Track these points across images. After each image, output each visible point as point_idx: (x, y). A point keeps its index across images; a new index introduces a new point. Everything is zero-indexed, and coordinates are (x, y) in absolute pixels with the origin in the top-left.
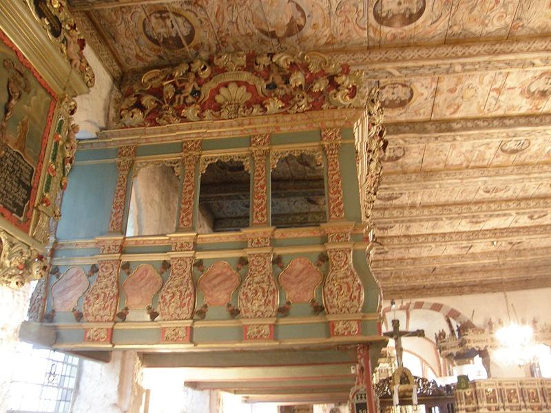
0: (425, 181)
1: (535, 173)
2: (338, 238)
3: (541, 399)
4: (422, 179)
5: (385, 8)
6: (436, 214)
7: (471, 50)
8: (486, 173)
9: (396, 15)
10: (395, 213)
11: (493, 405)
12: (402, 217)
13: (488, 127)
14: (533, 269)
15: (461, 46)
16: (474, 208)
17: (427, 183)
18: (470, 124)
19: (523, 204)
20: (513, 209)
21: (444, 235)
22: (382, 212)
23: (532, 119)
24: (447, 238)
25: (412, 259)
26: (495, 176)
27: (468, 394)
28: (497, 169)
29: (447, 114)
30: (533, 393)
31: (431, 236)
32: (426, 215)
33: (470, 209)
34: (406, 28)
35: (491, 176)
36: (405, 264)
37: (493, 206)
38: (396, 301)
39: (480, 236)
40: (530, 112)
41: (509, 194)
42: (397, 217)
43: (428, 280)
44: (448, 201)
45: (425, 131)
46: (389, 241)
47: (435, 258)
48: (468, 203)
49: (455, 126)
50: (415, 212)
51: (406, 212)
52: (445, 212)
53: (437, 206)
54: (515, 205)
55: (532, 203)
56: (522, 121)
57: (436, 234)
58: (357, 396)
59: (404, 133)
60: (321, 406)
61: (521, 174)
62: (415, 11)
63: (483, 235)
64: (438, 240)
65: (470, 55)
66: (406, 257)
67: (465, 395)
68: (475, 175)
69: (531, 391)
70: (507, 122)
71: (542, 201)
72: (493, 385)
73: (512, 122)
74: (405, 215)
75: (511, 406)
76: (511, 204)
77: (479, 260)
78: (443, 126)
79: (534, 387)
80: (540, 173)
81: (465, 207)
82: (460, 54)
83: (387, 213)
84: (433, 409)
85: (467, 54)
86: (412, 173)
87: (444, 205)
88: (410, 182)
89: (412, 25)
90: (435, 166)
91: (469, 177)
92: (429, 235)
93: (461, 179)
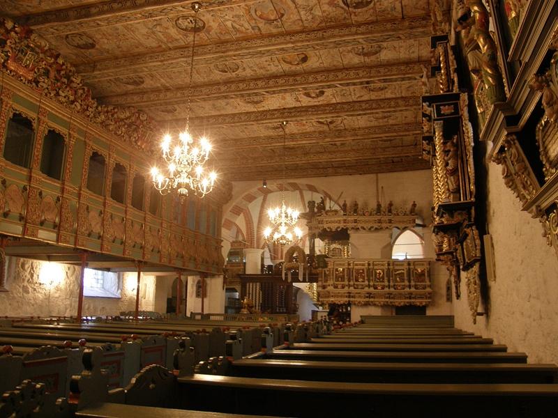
1: (231, 50)
3: (386, 278)
8: (186, 53)
10: (152, 96)
11: (340, 283)
12: (158, 100)
14: (380, 150)
16: (223, 88)
17: (133, 67)
18: (106, 8)
19: (271, 83)
20: (262, 88)
21: (234, 115)
22: (141, 96)
27: (327, 273)
30: (380, 274)
33: (219, 89)
37: (241, 86)
38: (268, 182)
39: (268, 117)
41: (248, 73)
42: (153, 100)
43: (273, 161)
45: (67, 18)
48: (218, 84)
49: (94, 10)
50: (169, 94)
51: (162, 96)
54: (264, 83)
55: (281, 81)
57: (227, 115)
60: (192, 277)
61: (219, 52)
67: (325, 273)
68: (175, 56)
69: (378, 272)
71: (291, 79)
72: (344, 265)
75: (357, 285)
76: (259, 82)
77: (297, 141)
78: (83, 12)
79: (382, 267)
80: (236, 50)
83: (145, 96)
86: (121, 58)
93: (162, 61)
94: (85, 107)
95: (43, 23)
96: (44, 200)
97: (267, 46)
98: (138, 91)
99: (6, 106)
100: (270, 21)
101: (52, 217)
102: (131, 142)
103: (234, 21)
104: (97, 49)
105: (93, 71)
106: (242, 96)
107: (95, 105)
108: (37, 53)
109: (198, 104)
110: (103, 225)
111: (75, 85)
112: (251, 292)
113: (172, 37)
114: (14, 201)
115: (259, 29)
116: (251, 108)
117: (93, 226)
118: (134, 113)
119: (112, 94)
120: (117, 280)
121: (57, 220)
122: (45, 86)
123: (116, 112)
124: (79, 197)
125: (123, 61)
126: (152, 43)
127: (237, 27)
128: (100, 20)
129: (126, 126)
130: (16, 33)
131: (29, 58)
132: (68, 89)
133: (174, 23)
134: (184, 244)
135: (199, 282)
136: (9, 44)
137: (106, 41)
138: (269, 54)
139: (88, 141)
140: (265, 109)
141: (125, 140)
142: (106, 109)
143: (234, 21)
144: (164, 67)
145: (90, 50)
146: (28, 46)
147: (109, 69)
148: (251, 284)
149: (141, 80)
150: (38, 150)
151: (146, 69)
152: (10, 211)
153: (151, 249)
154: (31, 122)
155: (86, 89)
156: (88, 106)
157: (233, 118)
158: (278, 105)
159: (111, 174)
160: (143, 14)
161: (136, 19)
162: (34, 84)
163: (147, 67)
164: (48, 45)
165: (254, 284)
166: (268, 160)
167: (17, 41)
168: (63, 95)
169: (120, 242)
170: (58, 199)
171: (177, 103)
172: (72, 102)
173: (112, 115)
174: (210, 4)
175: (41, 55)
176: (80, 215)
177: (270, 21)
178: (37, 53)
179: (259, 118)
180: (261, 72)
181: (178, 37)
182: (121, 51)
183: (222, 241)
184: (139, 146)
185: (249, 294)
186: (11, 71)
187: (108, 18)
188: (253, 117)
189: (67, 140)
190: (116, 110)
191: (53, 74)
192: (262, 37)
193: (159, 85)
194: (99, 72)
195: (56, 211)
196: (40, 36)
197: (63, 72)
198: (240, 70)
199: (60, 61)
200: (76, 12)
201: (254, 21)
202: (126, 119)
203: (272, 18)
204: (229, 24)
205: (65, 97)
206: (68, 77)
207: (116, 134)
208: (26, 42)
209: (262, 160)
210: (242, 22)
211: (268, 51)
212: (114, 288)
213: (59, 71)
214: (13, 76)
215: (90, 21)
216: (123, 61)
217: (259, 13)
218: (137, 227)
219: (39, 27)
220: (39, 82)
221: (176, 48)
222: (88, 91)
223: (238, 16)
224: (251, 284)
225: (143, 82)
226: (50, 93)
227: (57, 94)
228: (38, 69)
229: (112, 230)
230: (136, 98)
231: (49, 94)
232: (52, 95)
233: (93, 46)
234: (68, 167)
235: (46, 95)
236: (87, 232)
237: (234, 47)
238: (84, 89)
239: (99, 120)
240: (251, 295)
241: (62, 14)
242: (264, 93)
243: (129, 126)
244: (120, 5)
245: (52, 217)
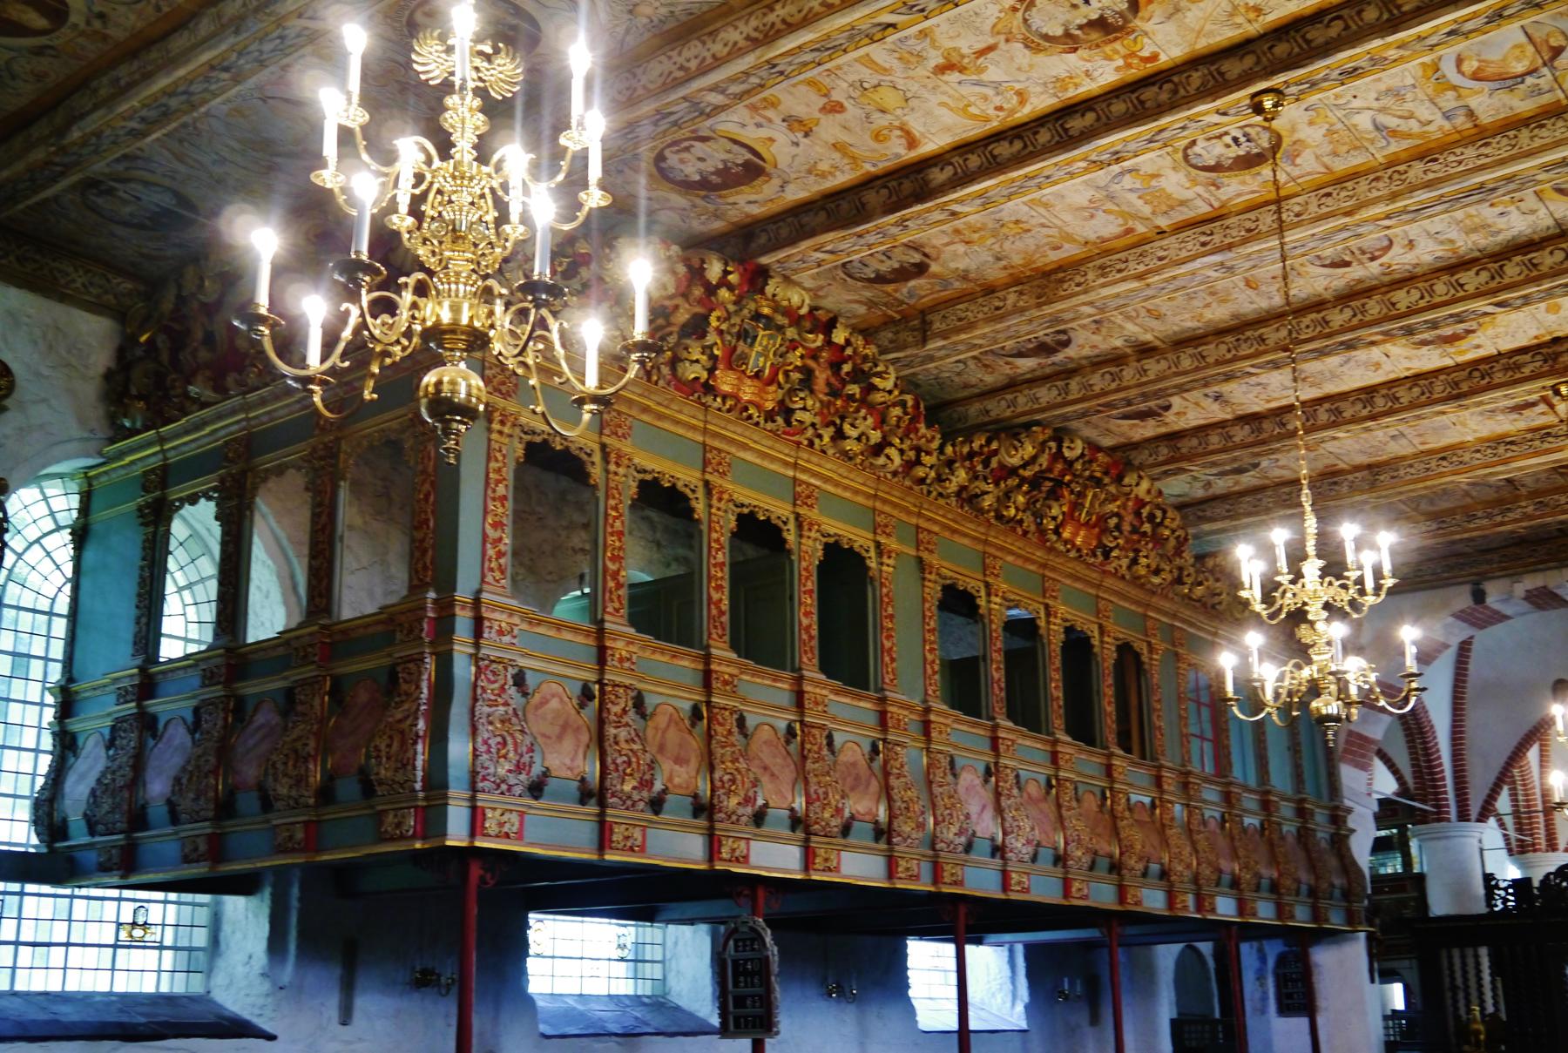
0: (1039, 306)
2: (411, 631)
4: (1033, 301)
6: (1218, 363)
7: (718, 48)
8: (1217, 238)
10: (1098, 381)
13: (1019, 160)
15: (698, 38)
17: (1047, 310)
18: (974, 161)
19: (1512, 270)
20: (1479, 294)
21: (1370, 391)
23: (1149, 94)
24: (1380, 403)
25: (1369, 467)
26: (1245, 241)
28: (1252, 215)
29: (898, 152)
31: (1327, 406)
32: (1185, 373)
35: (1230, 247)
36: (1345, 489)
37: (1403, 298)
39: (1499, 377)
40: (1134, 73)
42: (1104, 393)
43: (1511, 515)
44: (1360, 281)
45: (862, 215)
46: (1195, 442)
47: (1444, 453)
49: (938, 176)
50: (1153, 367)
51: (1128, 374)
52: (1245, 350)
53: (1220, 332)
56: (1118, 107)
57: (1343, 396)
58: (736, 941)
59: (812, 234)
63: (1506, 369)
64: (1347, 415)
65: (718, 62)
66: (1342, 466)
68: (1184, 254)
70: (1076, 124)
73: (1090, 117)
74: (1125, 384)
80: (1394, 197)
81: (1306, 320)
82: (693, 65)
83: (1074, 384)
84: (1444, 954)
85: (709, 60)
86: (1007, 286)
87: (1240, 328)
88: (1002, 318)
90: (1054, 257)
91: (1166, 262)
92: (1319, 401)
94: (912, 454)
95: (792, 241)
96: (842, 758)
97: (1502, 162)
98: (1048, 370)
100: (1510, 81)
101: (866, 805)
102: (1042, 532)
103: (1382, 110)
104: (935, 276)
105: (924, 341)
106: (1409, 331)
107: (935, 444)
108: (780, 329)
109: (1253, 380)
110: (999, 811)
111: (878, 397)
112: (1459, 981)
113: (1169, 197)
114: (773, 775)
115: (1471, 114)
116: (1431, 359)
117: (974, 817)
118: (1043, 444)
119: (966, 393)
120: (1008, 973)
121: (882, 814)
122: (807, 417)
123: (996, 452)
124: (927, 732)
125: (1012, 298)
126: (1105, 227)
127: (1392, 122)
128: (955, 201)
129: (1025, 488)
130: (731, 288)
131: (761, 353)
132: (863, 412)
133: (1180, 155)
134: (1232, 839)
135: (1281, 961)
136: (714, 323)
137: (961, 248)
138: (1512, 186)
139: (925, 555)
140: (1481, 353)
141: (1025, 533)
142: (966, 450)
143: (1382, 110)
144: (1149, 292)
145: (912, 283)
146: (757, 316)
147: (971, 326)
148: (1456, 953)
149: (1064, 337)
150: (806, 614)
151: (1087, 310)
153: (1140, 866)
154: (686, 499)
155: (910, 403)
156: (918, 450)
157: (1370, 402)
158: (1534, 332)
159: (999, 644)
160: (1093, 157)
161: (1072, 175)
163: (1091, 303)
164: (807, 301)
165: (1470, 952)
166: (1489, 516)
167: (731, 308)
168: (854, 433)
169: (1050, 858)
170: (875, 750)
171: (1182, 389)
172: (878, 450)
173: (986, 464)
174: (1313, 84)
175: (791, 333)
176: (937, 790)
177: (1510, 81)
178: (780, 329)
179: (1465, 387)
180: (1466, 243)
181: (1189, 194)
182: (1005, 268)
183: (1349, 811)
184: (1066, 542)
185: (1454, 988)
186: (724, 398)
187: (986, 190)
188: (1439, 389)
189: (873, 564)
190: (994, 446)
191: (822, 376)
192: (1481, 135)
193: (1118, 343)
194: (941, 343)
195: (875, 786)
196: (787, 279)
197: (847, 368)
198: (1396, 250)
199: (839, 336)
200: (884, 192)
201: (1451, 94)
202: (1024, 466)
203: (1520, 68)
204: (1364, 121)
205: (859, 439)
207: (999, 517)
208: (752, 306)
209: (1471, 517)
210: (1408, 106)
211: (1509, 179)
212: (999, 997)
213: (835, 366)
215: (929, 211)
216: (1012, 298)
217: (1470, 66)
218: (1091, 803)
219: (781, 255)
220: (793, 411)
221: (1180, 228)
222: (916, 406)
223: (1396, 94)
224: (1456, 953)
225: (1067, 343)
227: (839, 435)
228: (786, 374)
229: (1026, 825)
230: (1046, 394)
231: (817, 441)
232: (826, 439)
233: (920, 269)
234: (887, 644)
236: (963, 839)
237: (1383, 188)
238: (903, 404)
239: (952, 487)
240: (1461, 995)
241: (845, 205)
242: (1490, 309)
243: (1035, 482)
244: (1018, 145)
245: (866, 805)
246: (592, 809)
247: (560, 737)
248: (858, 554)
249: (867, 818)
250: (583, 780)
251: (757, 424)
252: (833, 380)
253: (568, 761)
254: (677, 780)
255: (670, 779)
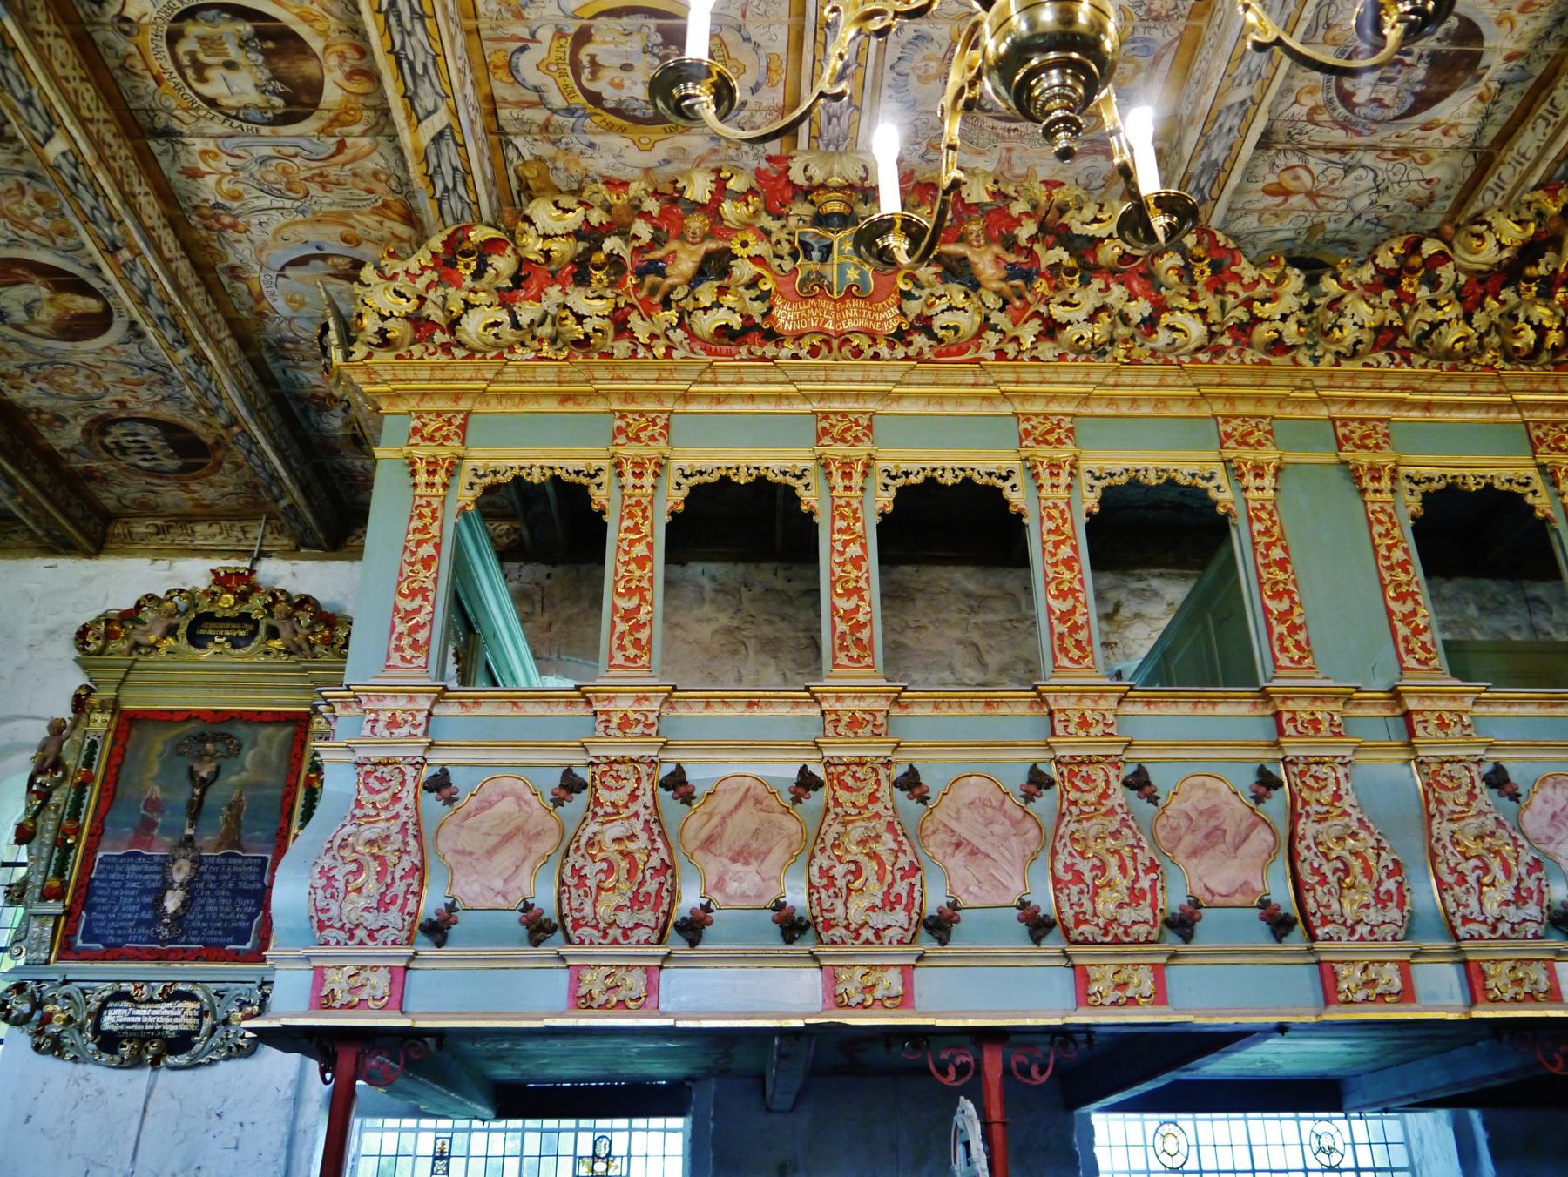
5: (254, 97)
9: (272, 71)
34: (317, 45)
62: (246, 28)
89: (302, 30)
99: (847, 475)
114: (974, 852)
142: (1367, 273)
146: (821, 220)
152: (954, 906)
162: (920, 340)
168: (1080, 314)
172: (1150, 324)
205: (1092, 319)
206: (1064, 237)
214: (814, 352)
226: (1016, 339)
227: (1051, 329)
231: (1011, 349)
235: (1001, 354)
246: (1296, 941)
247: (491, 852)
248: (1193, 488)
249: (1239, 899)
250: (527, 907)
251: (876, 356)
252: (1012, 258)
253: (498, 884)
254: (733, 887)
255: (720, 885)
